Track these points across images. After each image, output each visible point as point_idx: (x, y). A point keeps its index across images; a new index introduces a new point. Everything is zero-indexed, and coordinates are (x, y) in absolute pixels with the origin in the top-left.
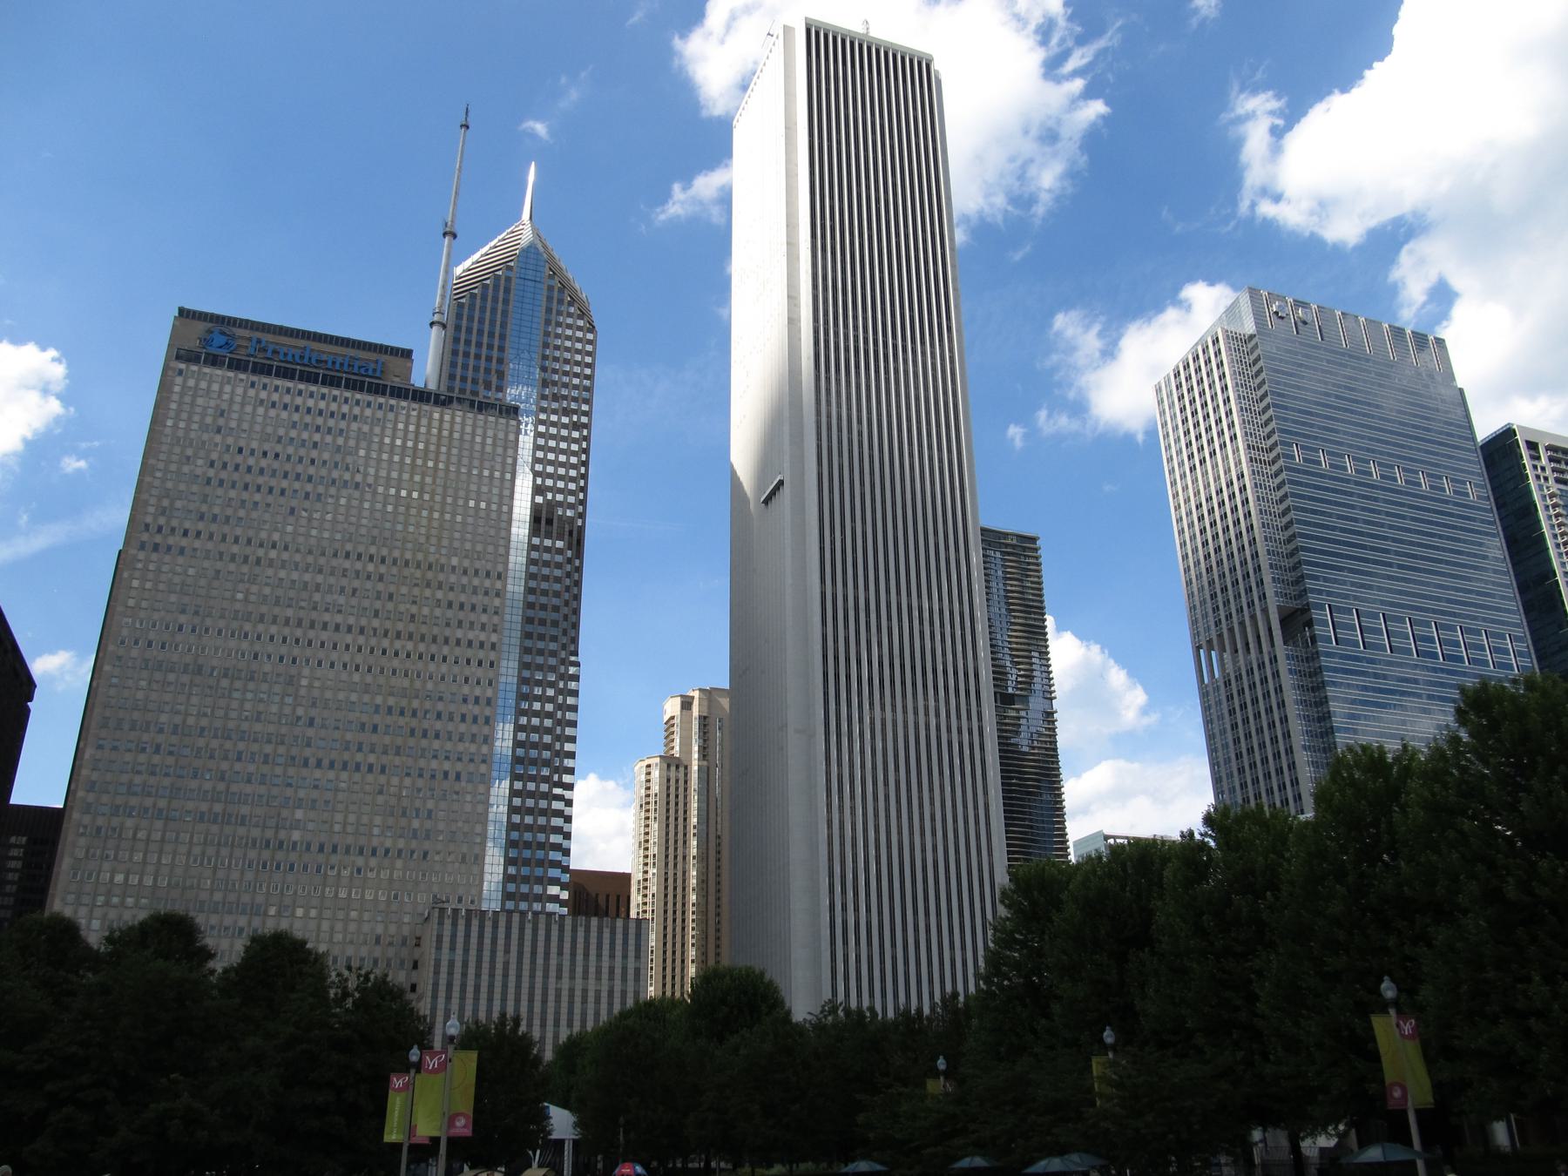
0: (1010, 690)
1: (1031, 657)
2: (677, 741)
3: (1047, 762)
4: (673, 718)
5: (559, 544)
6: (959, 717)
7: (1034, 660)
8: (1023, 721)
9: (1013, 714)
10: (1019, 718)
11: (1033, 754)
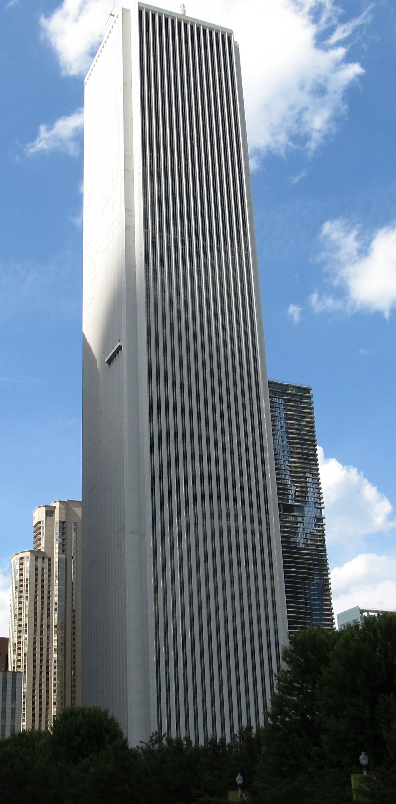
0: (290, 502)
2: (43, 540)
3: (318, 555)
4: (39, 522)
6: (252, 522)
7: (308, 480)
8: (300, 525)
9: (292, 519)
10: (297, 523)
11: (308, 550)
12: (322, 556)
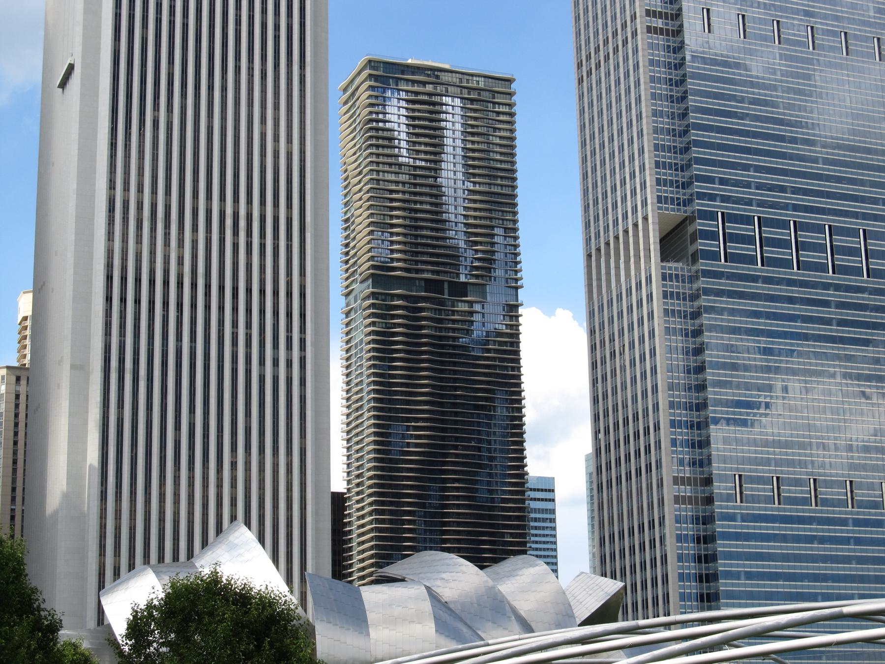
0: (463, 279)
1: (493, 236)
2: (29, 348)
3: (506, 368)
4: (25, 318)
6: (276, 346)
7: (496, 239)
10: (471, 313)
11: (487, 359)
12: (513, 369)
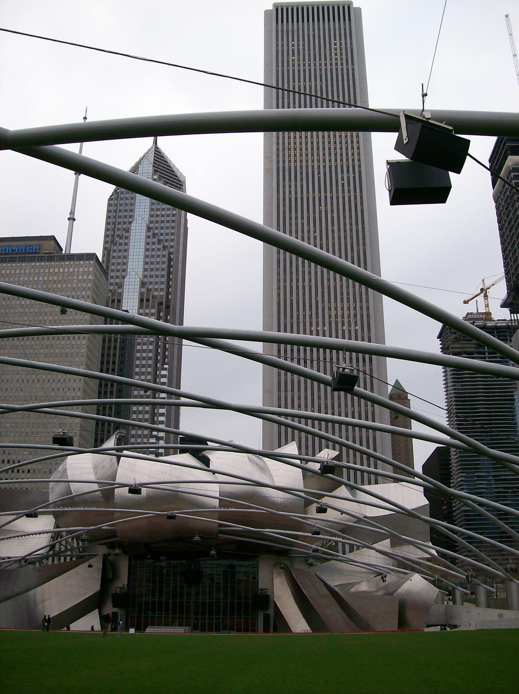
5: (153, 311)
